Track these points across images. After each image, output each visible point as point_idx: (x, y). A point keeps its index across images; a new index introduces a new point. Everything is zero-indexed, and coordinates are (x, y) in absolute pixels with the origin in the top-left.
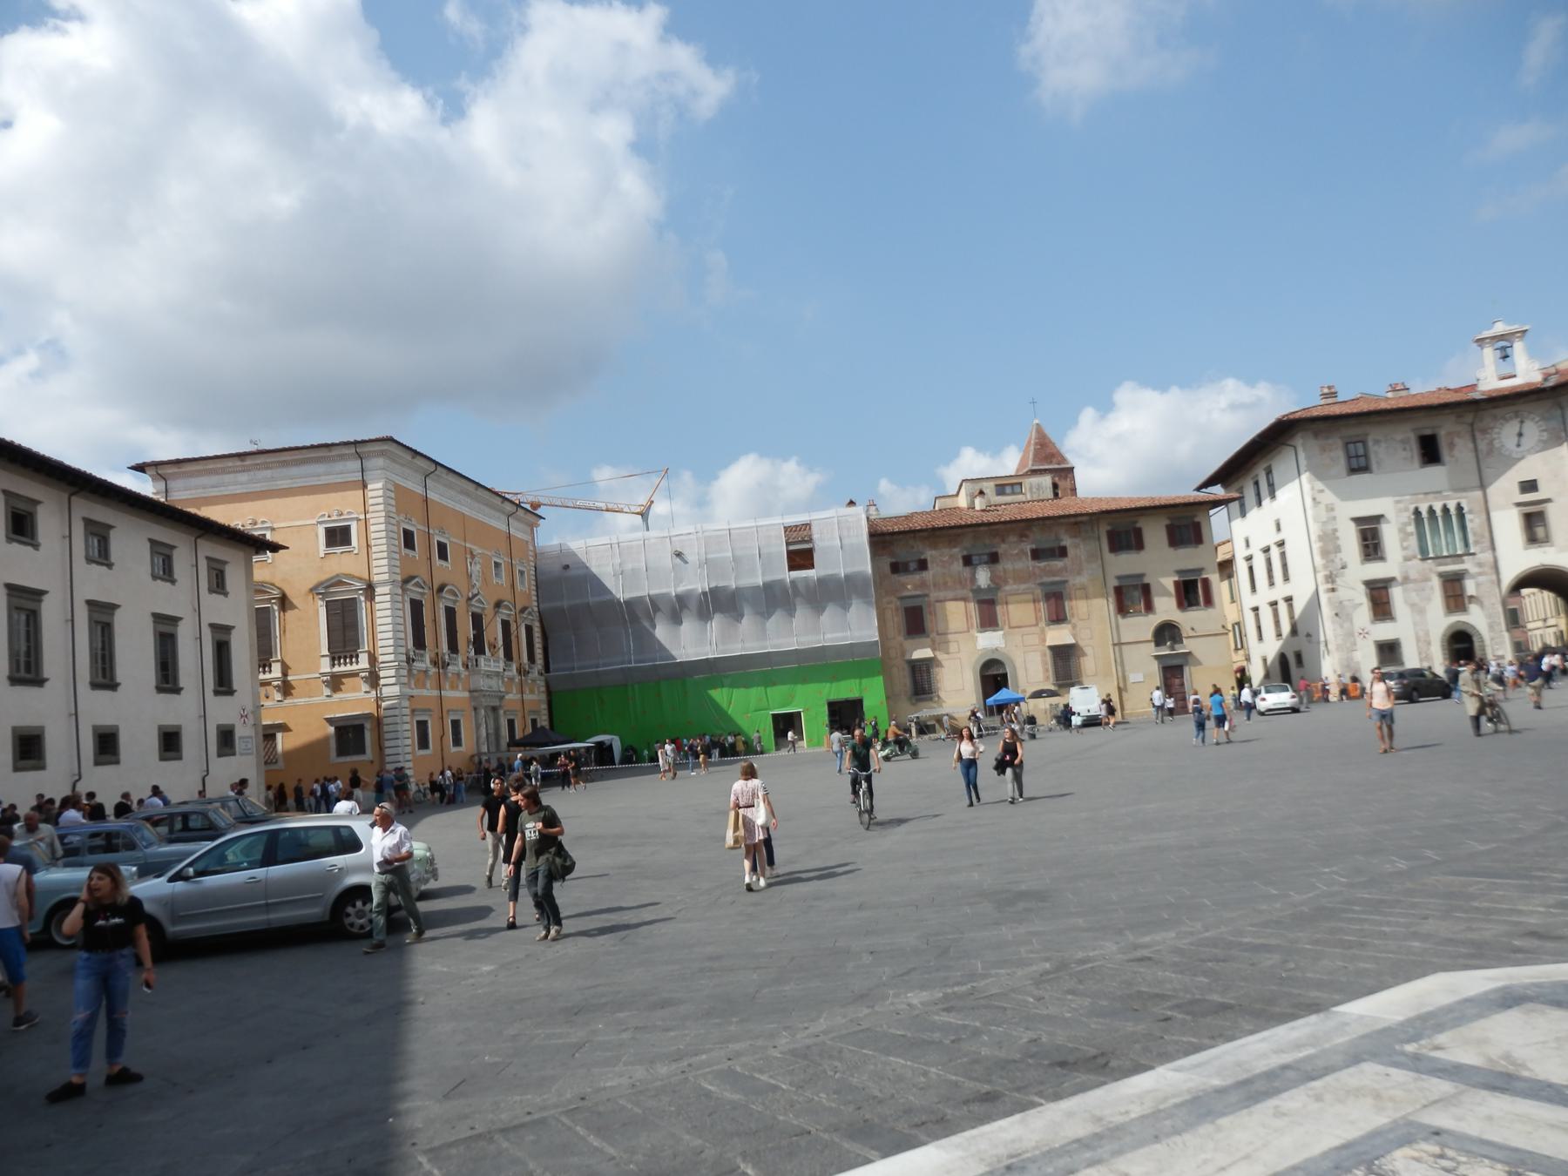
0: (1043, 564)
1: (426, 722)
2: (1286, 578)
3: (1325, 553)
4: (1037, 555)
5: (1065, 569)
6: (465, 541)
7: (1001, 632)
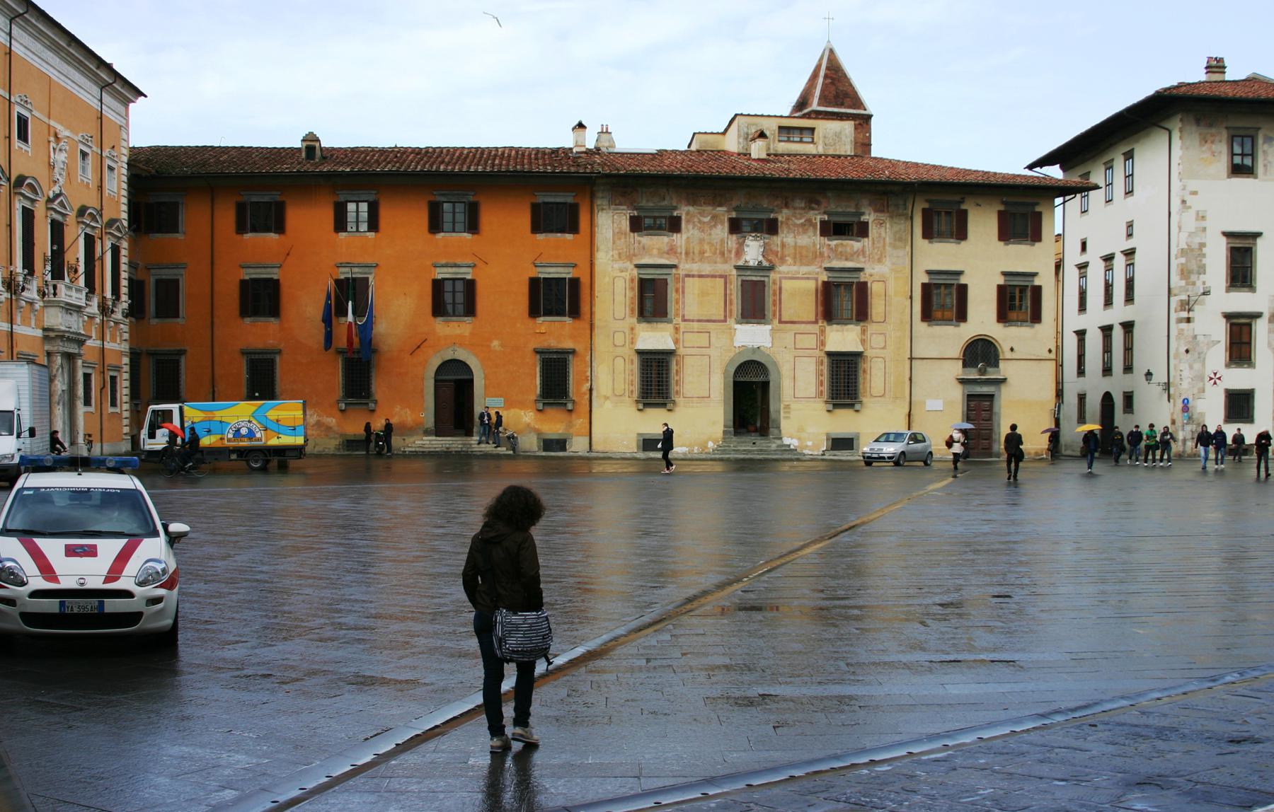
0: (834, 243)
1: (116, 377)
2: (1129, 298)
3: (1185, 273)
5: (862, 252)
6: (49, 118)
7: (769, 327)
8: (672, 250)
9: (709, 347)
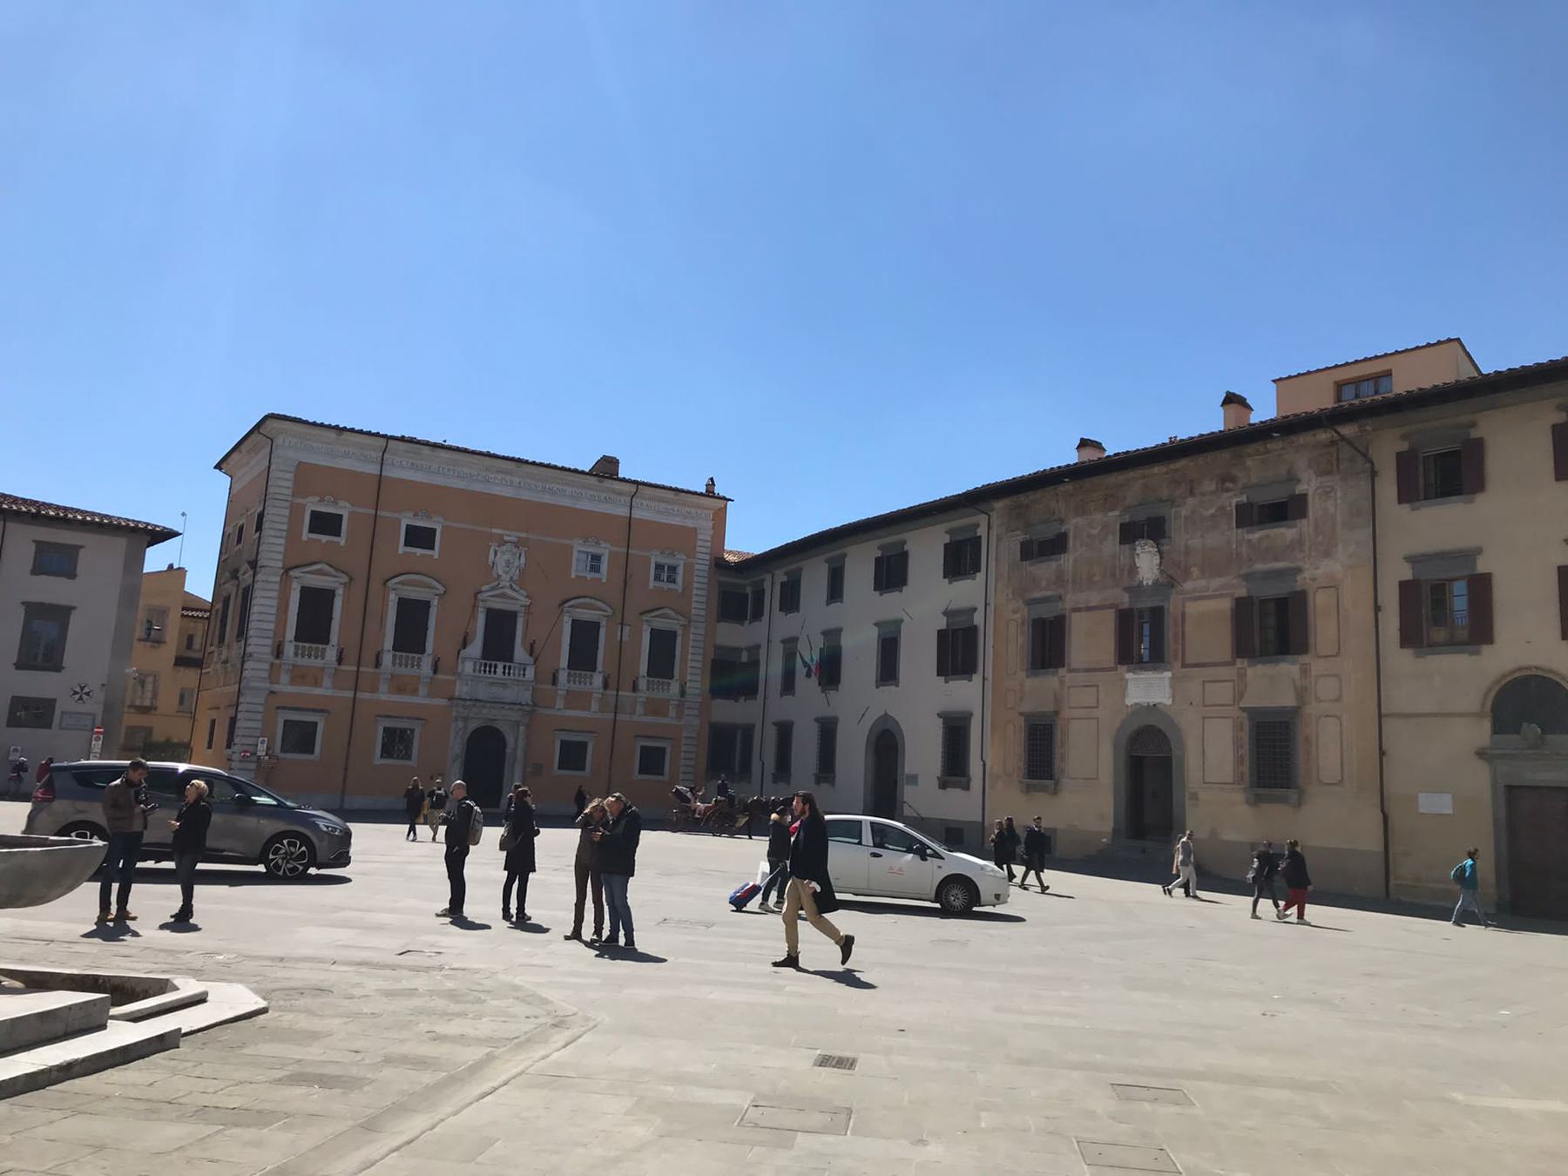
0: (1256, 535)
4: (1249, 516)
5: (1299, 543)
7: (1168, 674)
8: (1060, 579)
9: (1097, 707)
